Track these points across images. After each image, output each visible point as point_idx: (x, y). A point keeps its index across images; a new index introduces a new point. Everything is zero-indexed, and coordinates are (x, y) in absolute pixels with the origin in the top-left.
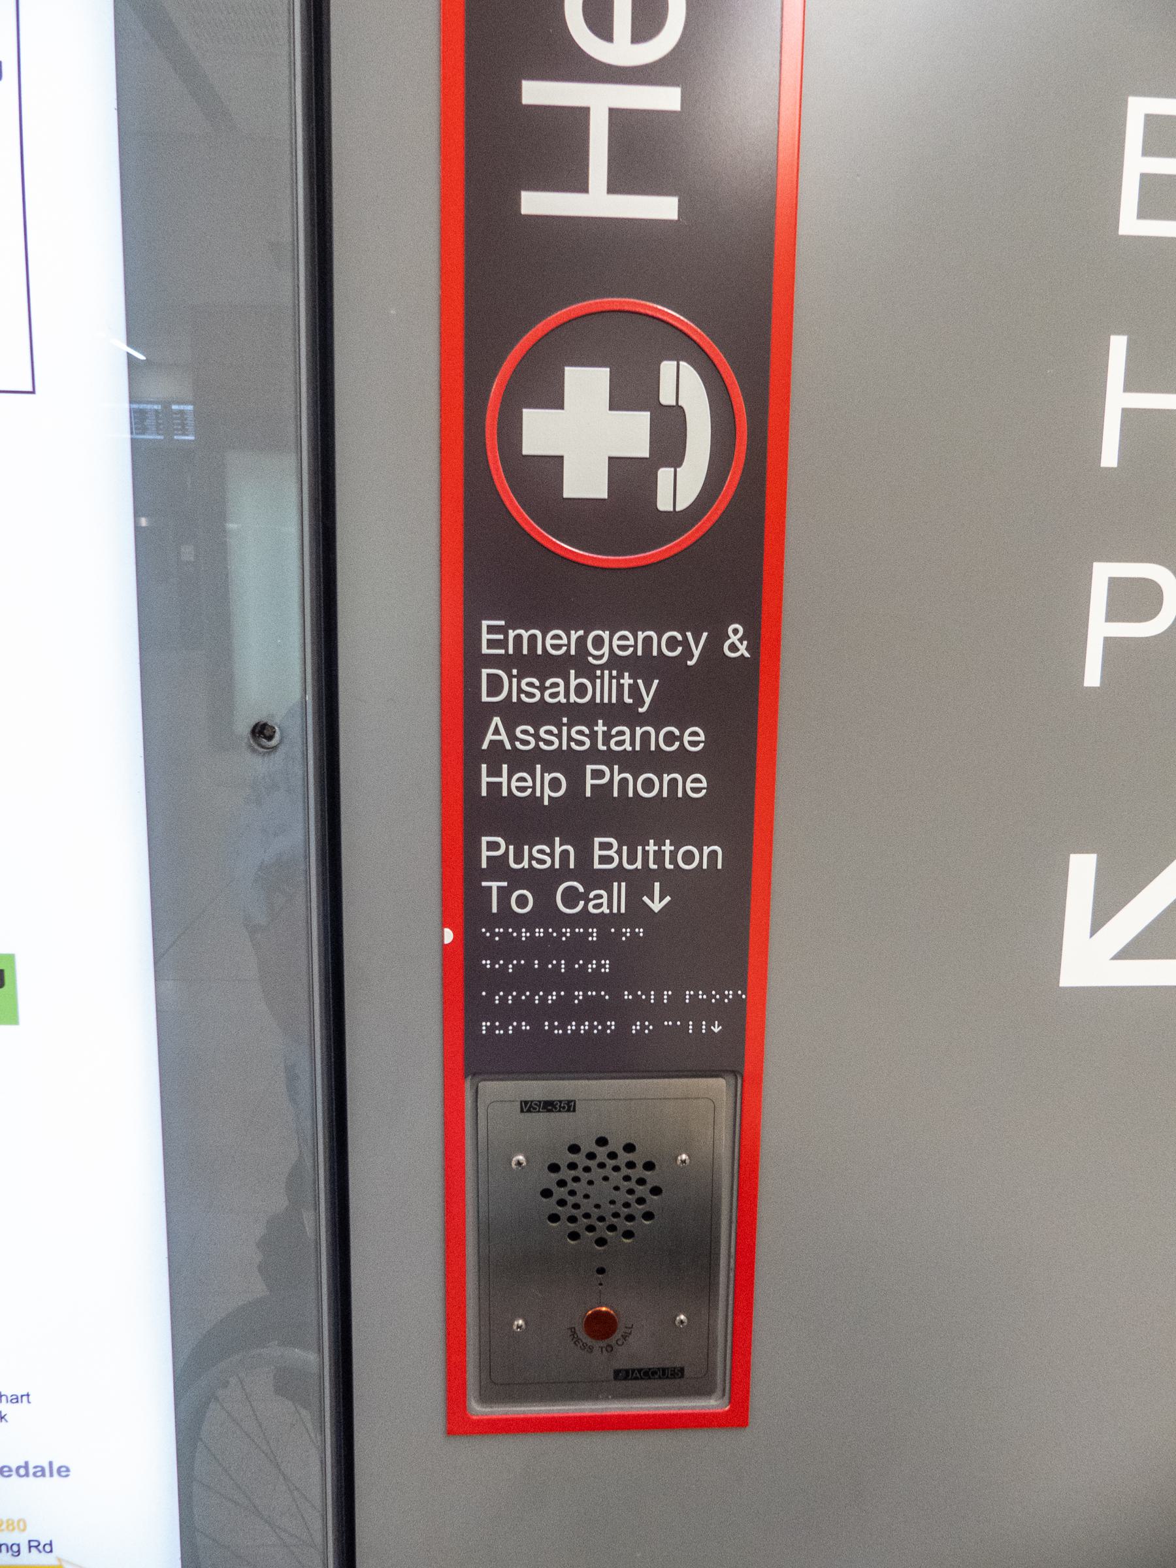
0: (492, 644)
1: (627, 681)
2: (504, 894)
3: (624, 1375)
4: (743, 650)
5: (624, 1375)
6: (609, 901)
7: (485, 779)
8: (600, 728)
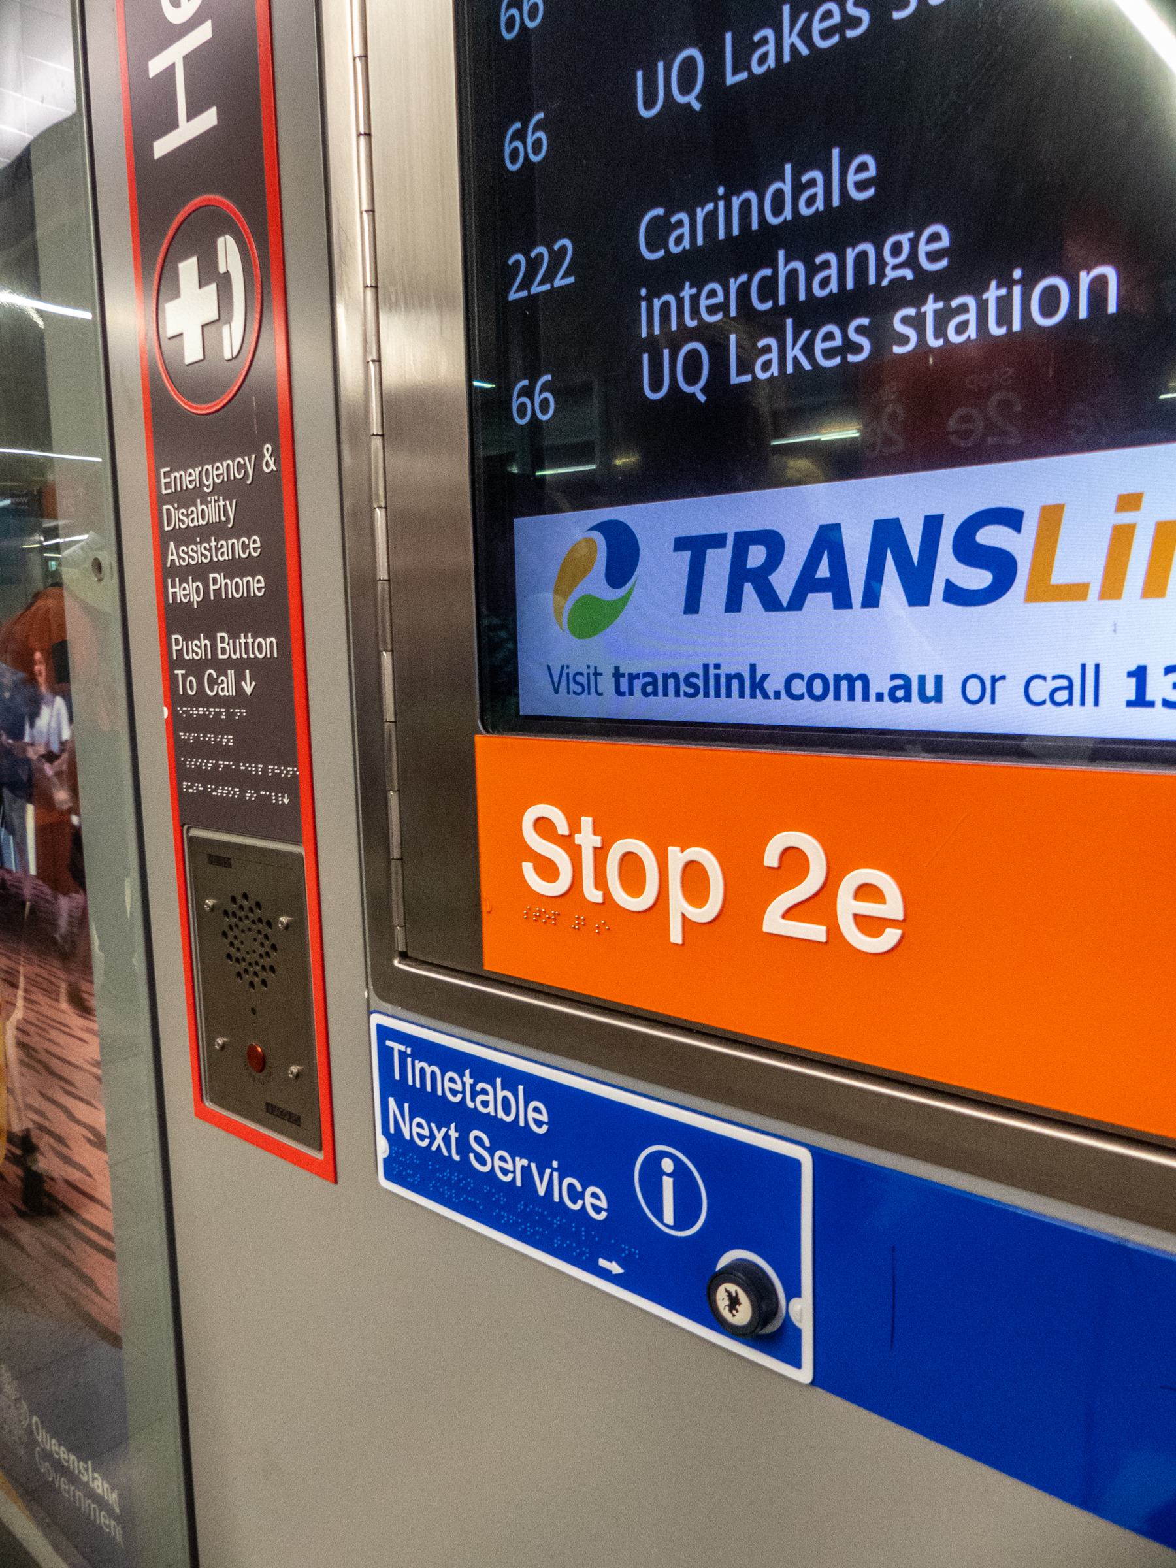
0: (167, 485)
1: (222, 503)
2: (184, 677)
3: (271, 1108)
4: (273, 467)
5: (271, 1108)
6: (227, 687)
7: (171, 590)
8: (213, 544)
